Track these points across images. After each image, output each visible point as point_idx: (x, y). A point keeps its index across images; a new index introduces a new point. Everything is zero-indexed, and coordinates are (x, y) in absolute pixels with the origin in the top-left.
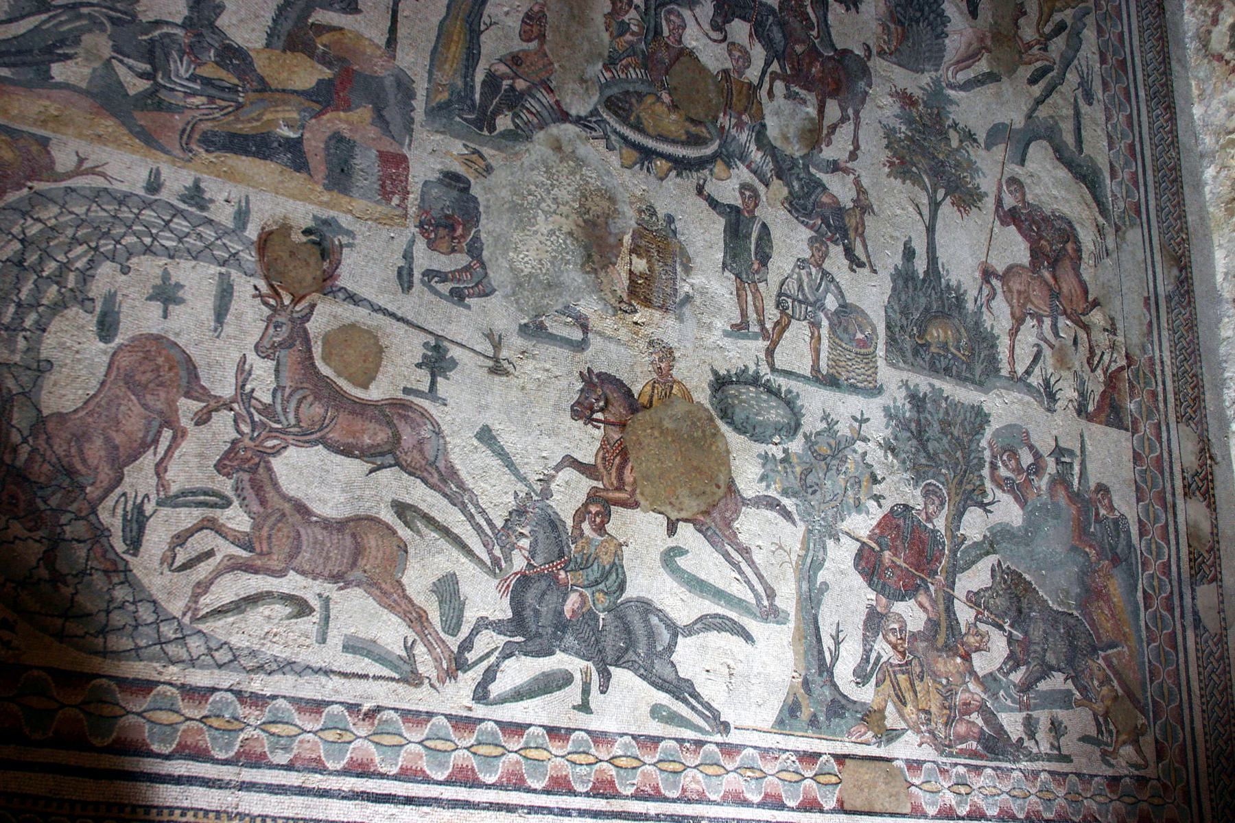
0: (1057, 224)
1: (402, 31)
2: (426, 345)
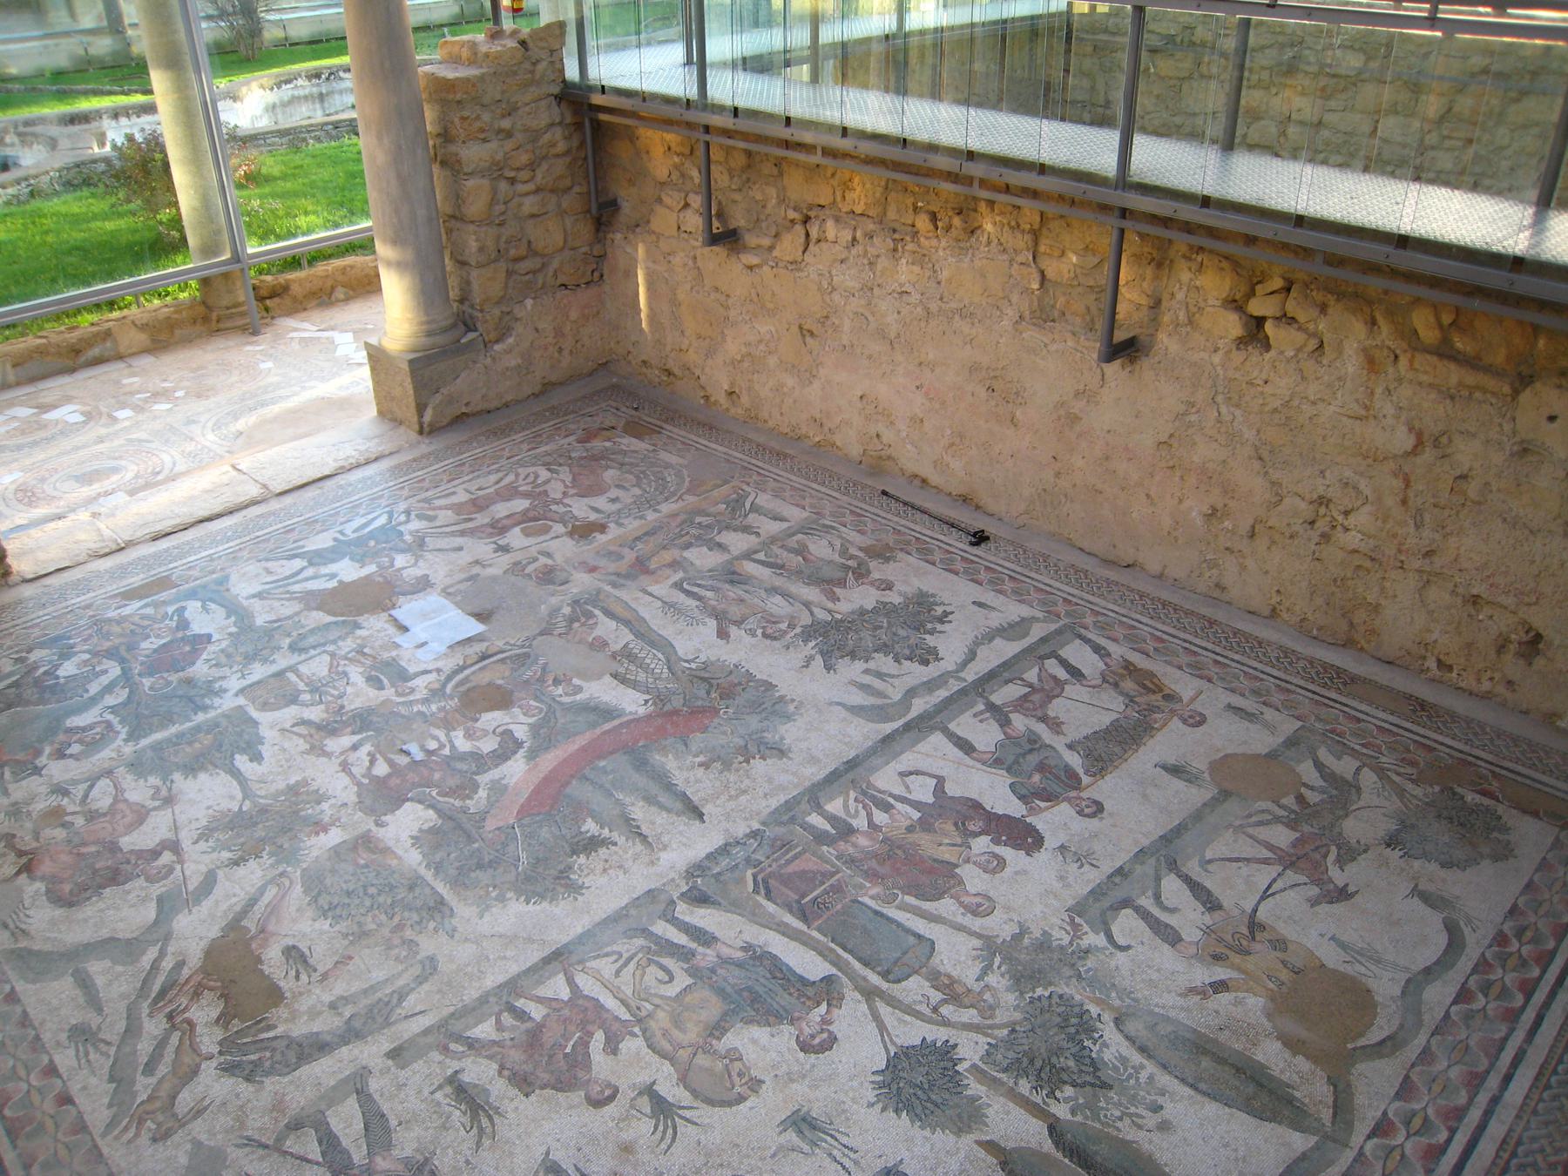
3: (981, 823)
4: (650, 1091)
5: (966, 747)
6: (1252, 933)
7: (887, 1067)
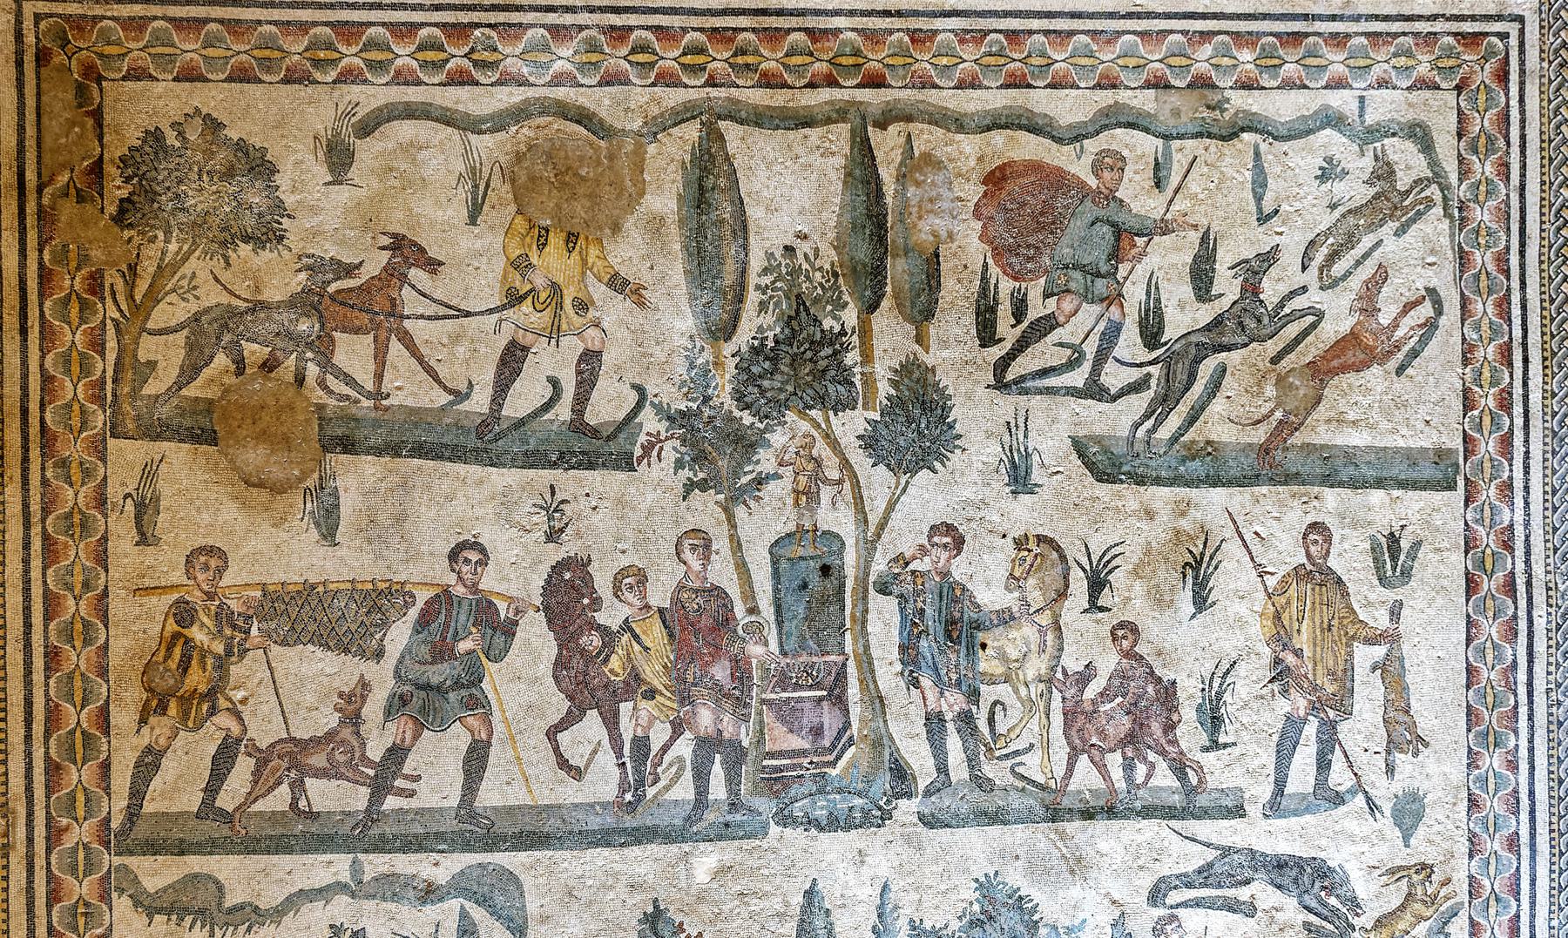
3: (584, 640)
4: (1094, 606)
5: (476, 761)
6: (522, 299)
7: (921, 468)
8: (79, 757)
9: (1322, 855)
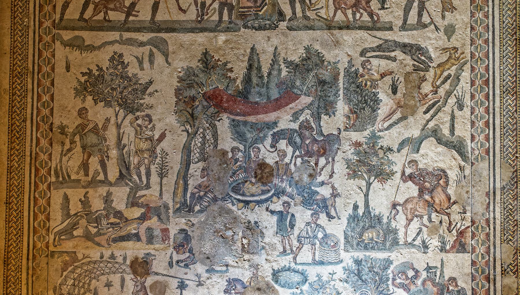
0: (436, 173)
1: (164, 189)
2: (178, 282)
8: (48, 3)
9: (420, 43)
